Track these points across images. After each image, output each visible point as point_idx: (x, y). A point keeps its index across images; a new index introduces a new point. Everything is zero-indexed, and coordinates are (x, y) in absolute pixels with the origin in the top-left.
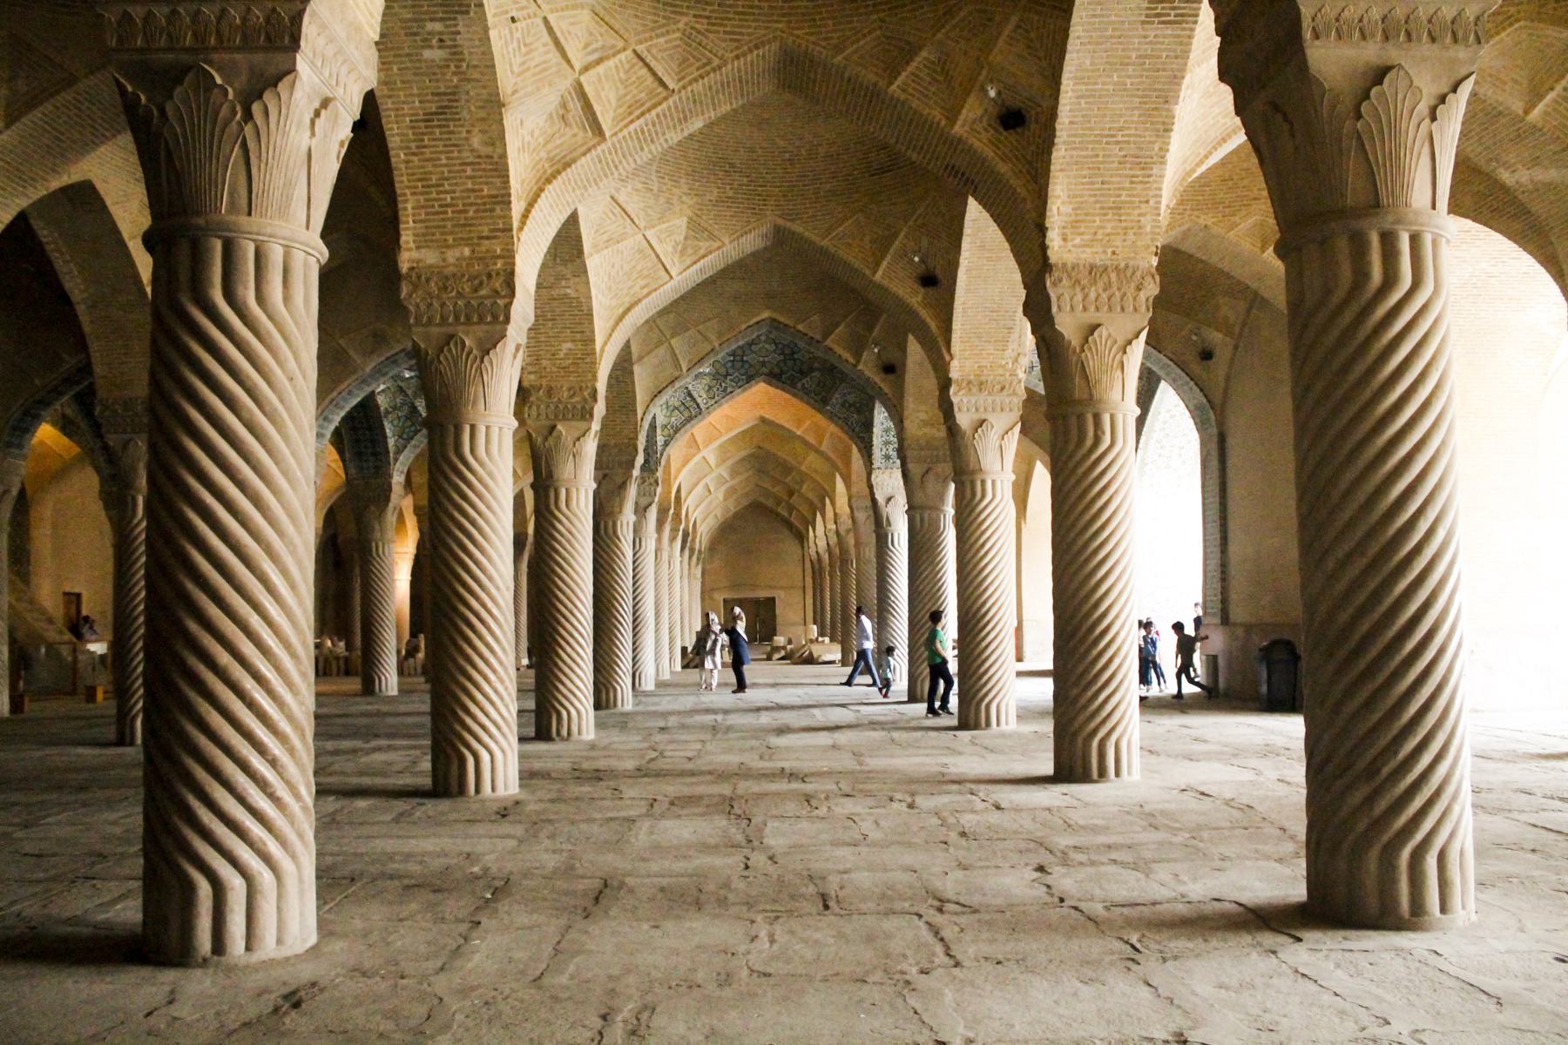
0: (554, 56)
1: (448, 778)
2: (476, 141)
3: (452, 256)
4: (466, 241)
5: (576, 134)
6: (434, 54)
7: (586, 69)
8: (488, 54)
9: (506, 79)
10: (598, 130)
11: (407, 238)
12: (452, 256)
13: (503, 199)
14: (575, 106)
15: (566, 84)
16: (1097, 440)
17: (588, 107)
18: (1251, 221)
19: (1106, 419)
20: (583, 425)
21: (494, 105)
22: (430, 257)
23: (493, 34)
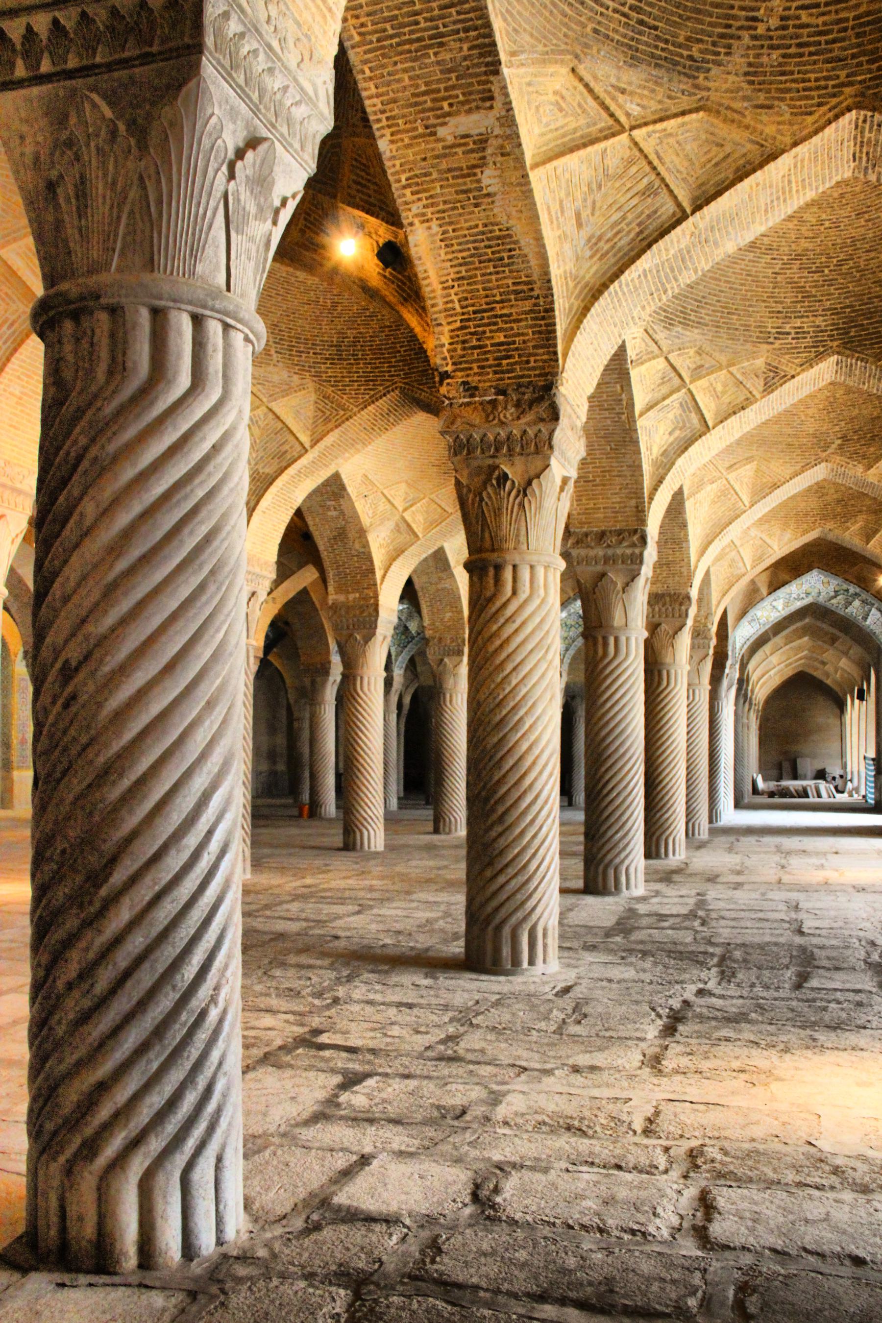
0: (388, 506)
1: (350, 842)
2: (357, 546)
3: (351, 597)
4: (357, 590)
5: (405, 537)
6: (334, 513)
7: (405, 510)
8: (356, 512)
9: (366, 520)
10: (417, 536)
11: (331, 589)
12: (351, 597)
13: (372, 571)
14: (403, 526)
15: (397, 517)
16: (659, 684)
17: (409, 525)
18: (858, 526)
19: (665, 673)
20: (457, 659)
21: (362, 533)
22: (341, 598)
23: (357, 505)
